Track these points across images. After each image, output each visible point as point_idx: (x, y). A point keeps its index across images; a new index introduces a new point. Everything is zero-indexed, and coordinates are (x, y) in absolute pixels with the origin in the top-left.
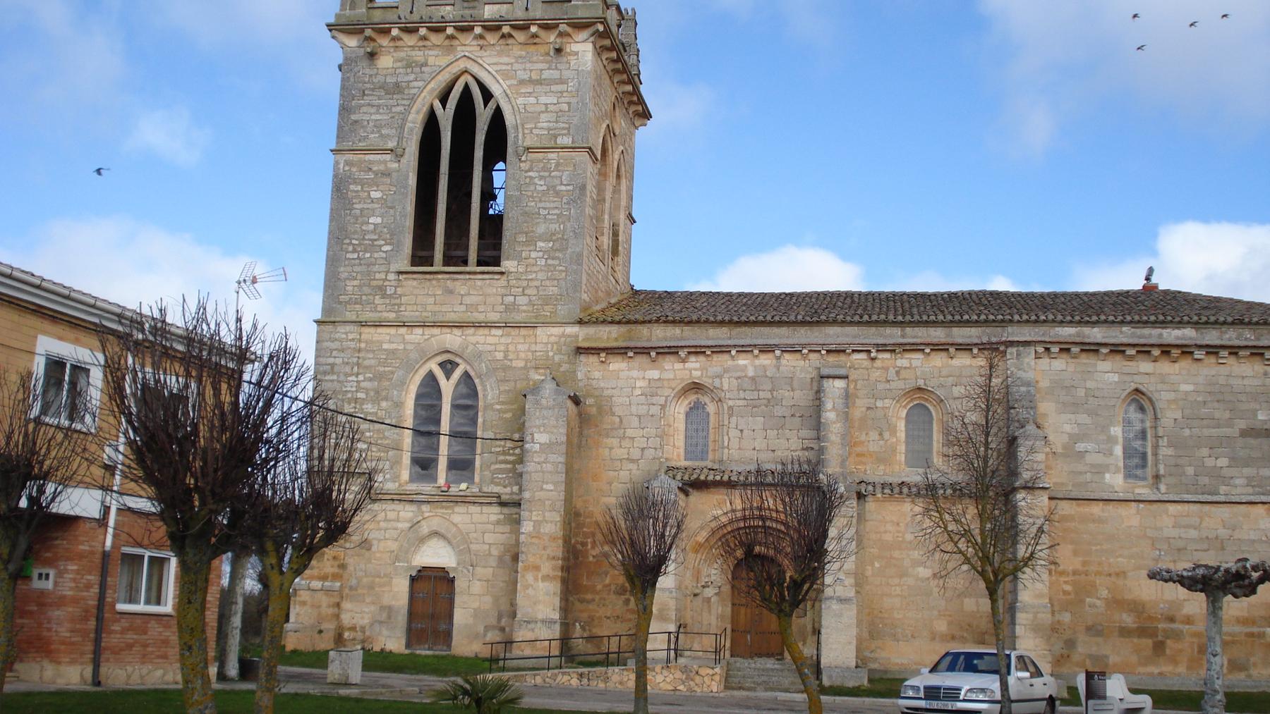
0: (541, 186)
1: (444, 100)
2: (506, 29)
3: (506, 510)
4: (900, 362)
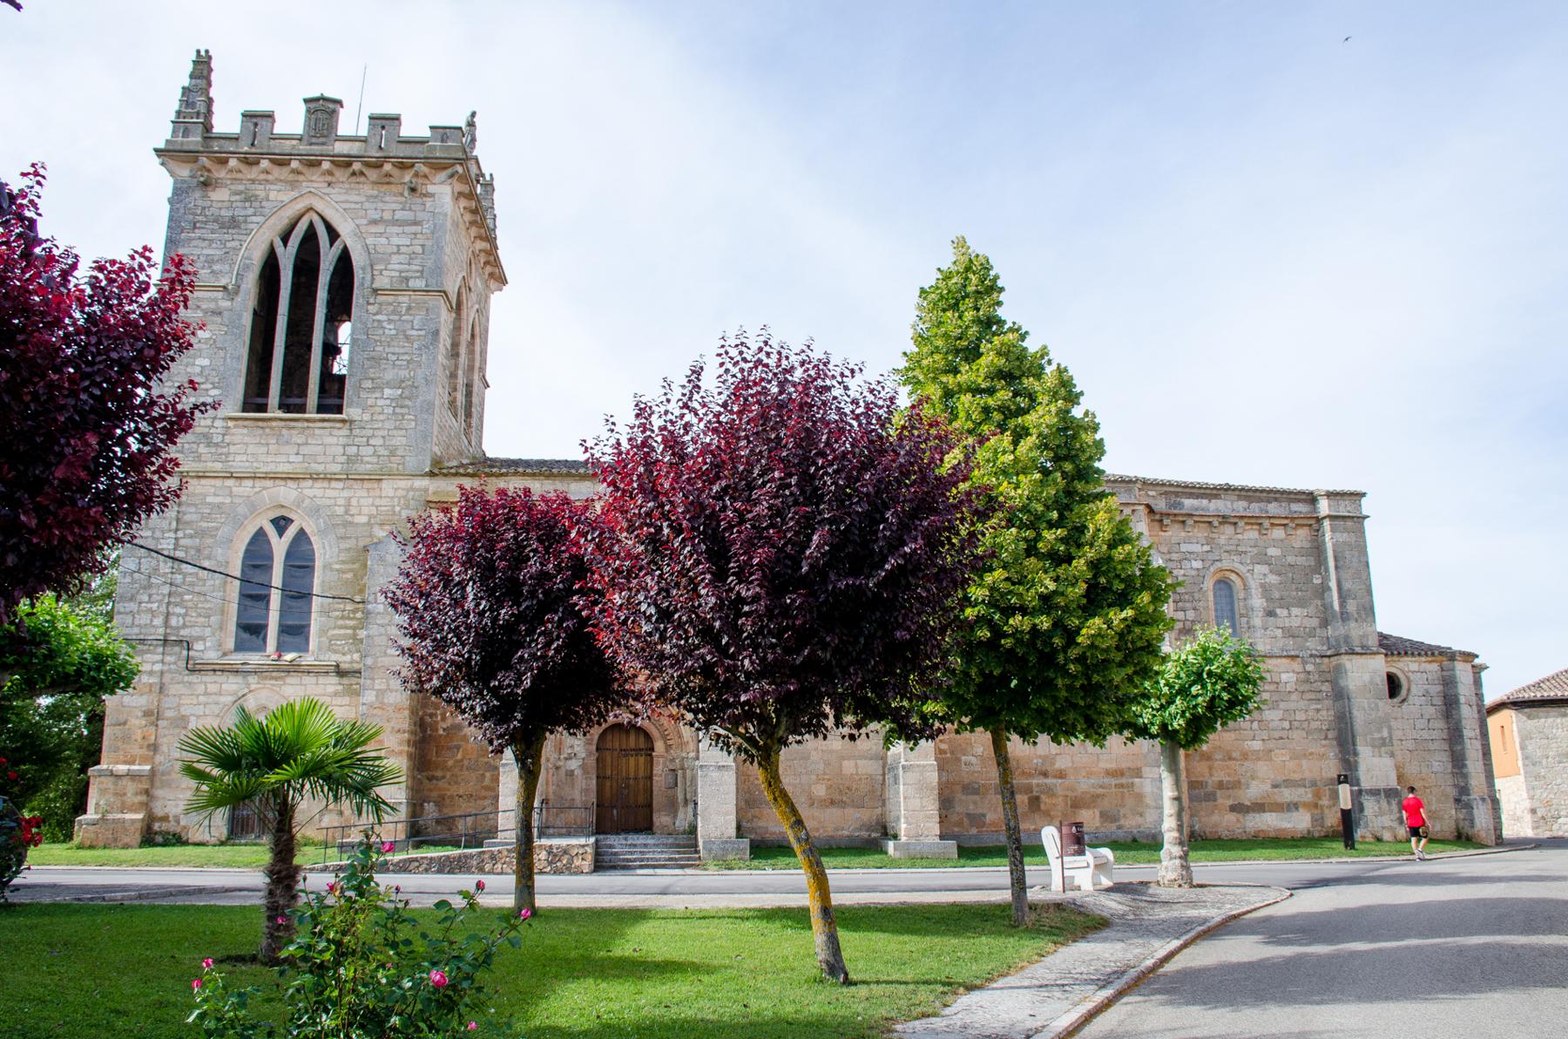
0: (390, 329)
1: (285, 239)
2: (357, 166)
3: (345, 681)
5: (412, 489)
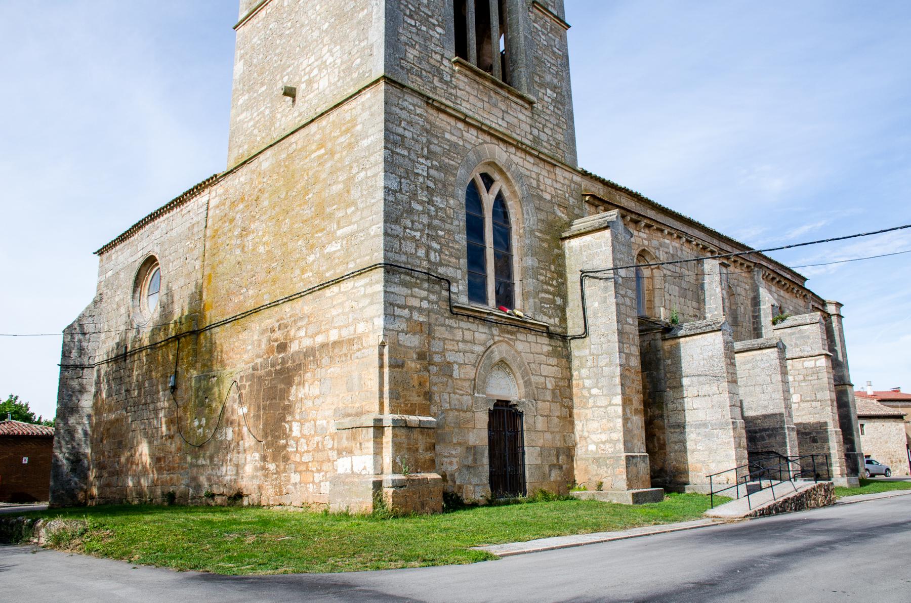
5: (572, 181)
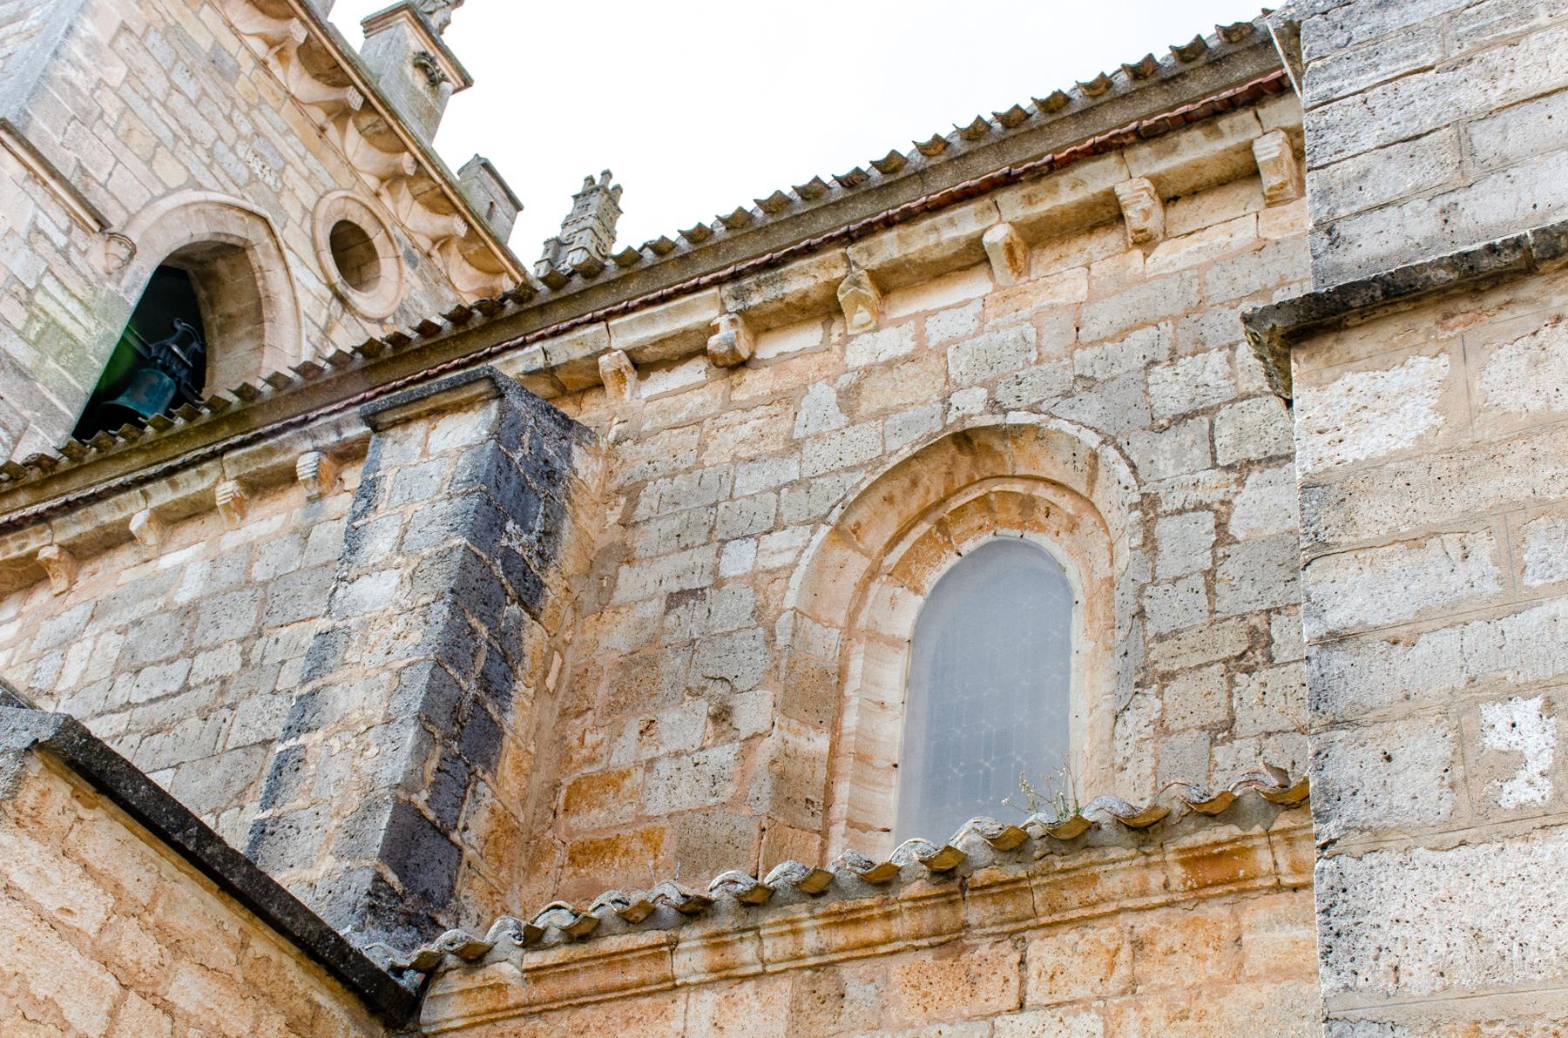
4: (860, 353)
